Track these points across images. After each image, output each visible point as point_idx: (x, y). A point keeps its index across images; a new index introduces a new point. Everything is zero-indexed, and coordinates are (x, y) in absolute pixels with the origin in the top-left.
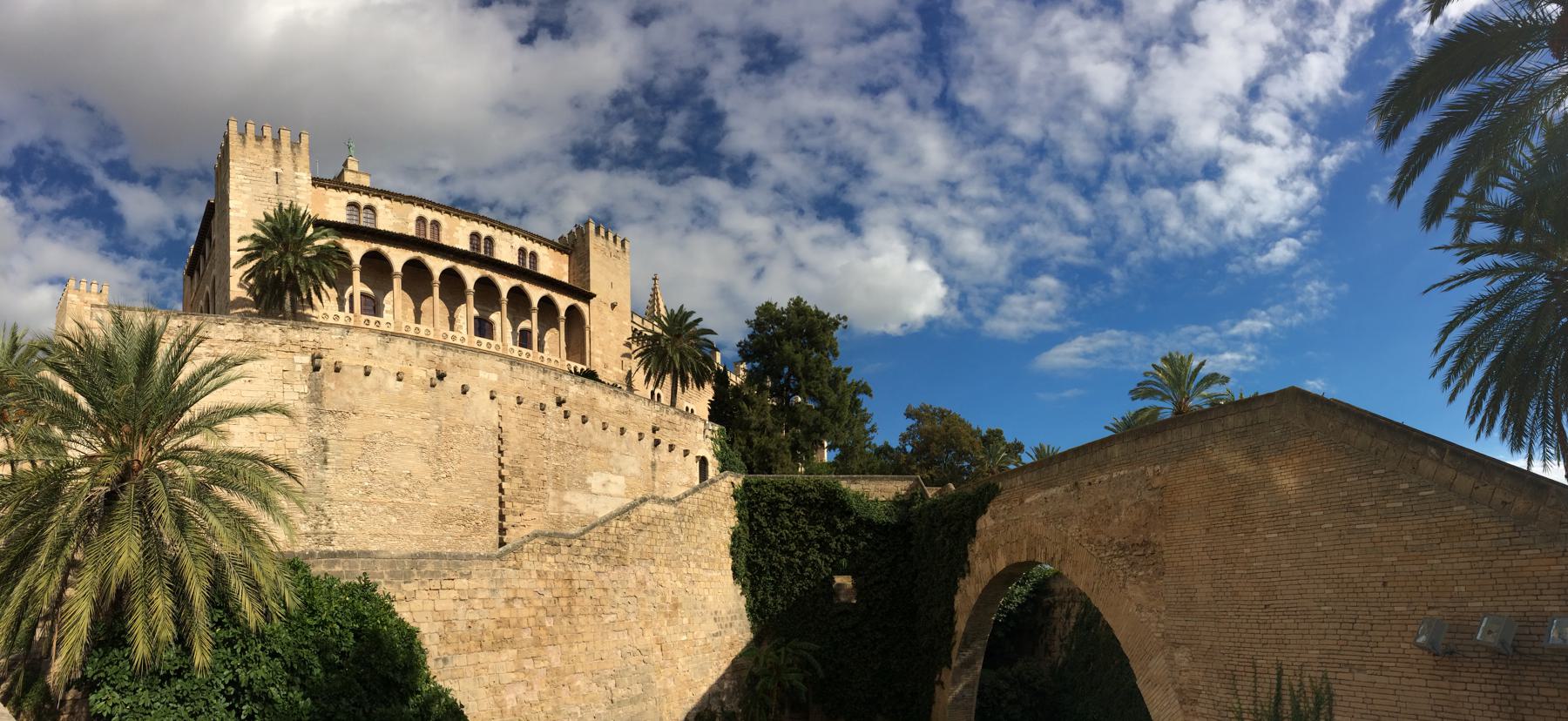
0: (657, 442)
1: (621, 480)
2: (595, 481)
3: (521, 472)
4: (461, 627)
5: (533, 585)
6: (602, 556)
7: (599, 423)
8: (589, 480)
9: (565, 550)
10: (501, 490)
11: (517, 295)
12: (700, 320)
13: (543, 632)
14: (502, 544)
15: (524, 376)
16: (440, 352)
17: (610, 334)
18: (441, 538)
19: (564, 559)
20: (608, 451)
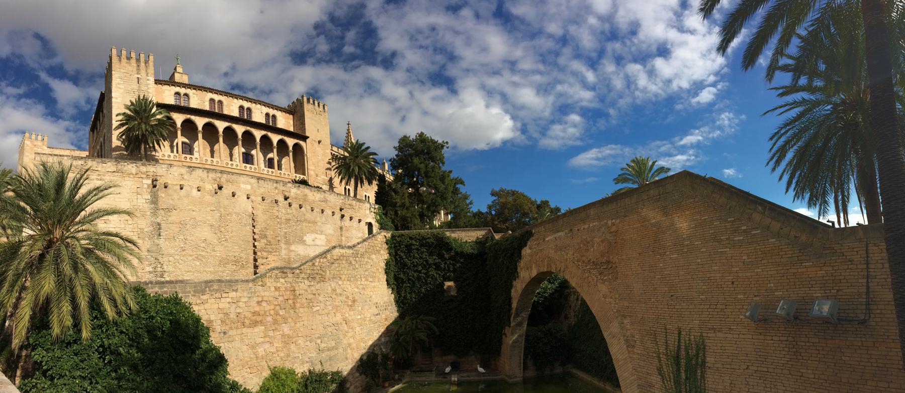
0: (343, 216)
1: (323, 237)
2: (308, 238)
3: (265, 237)
4: (233, 316)
5: (272, 294)
6: (311, 277)
7: (309, 208)
8: (305, 238)
9: (290, 275)
10: (255, 246)
11: (265, 140)
12: (368, 148)
13: (278, 317)
14: (255, 273)
15: (266, 186)
16: (219, 175)
17: (319, 156)
18: (223, 272)
19: (290, 280)
20: (315, 223)
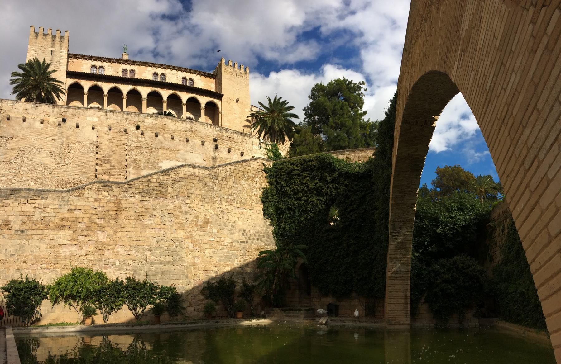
5: (91, 204)
7: (168, 137)
16: (65, 110)
19: (115, 193)
